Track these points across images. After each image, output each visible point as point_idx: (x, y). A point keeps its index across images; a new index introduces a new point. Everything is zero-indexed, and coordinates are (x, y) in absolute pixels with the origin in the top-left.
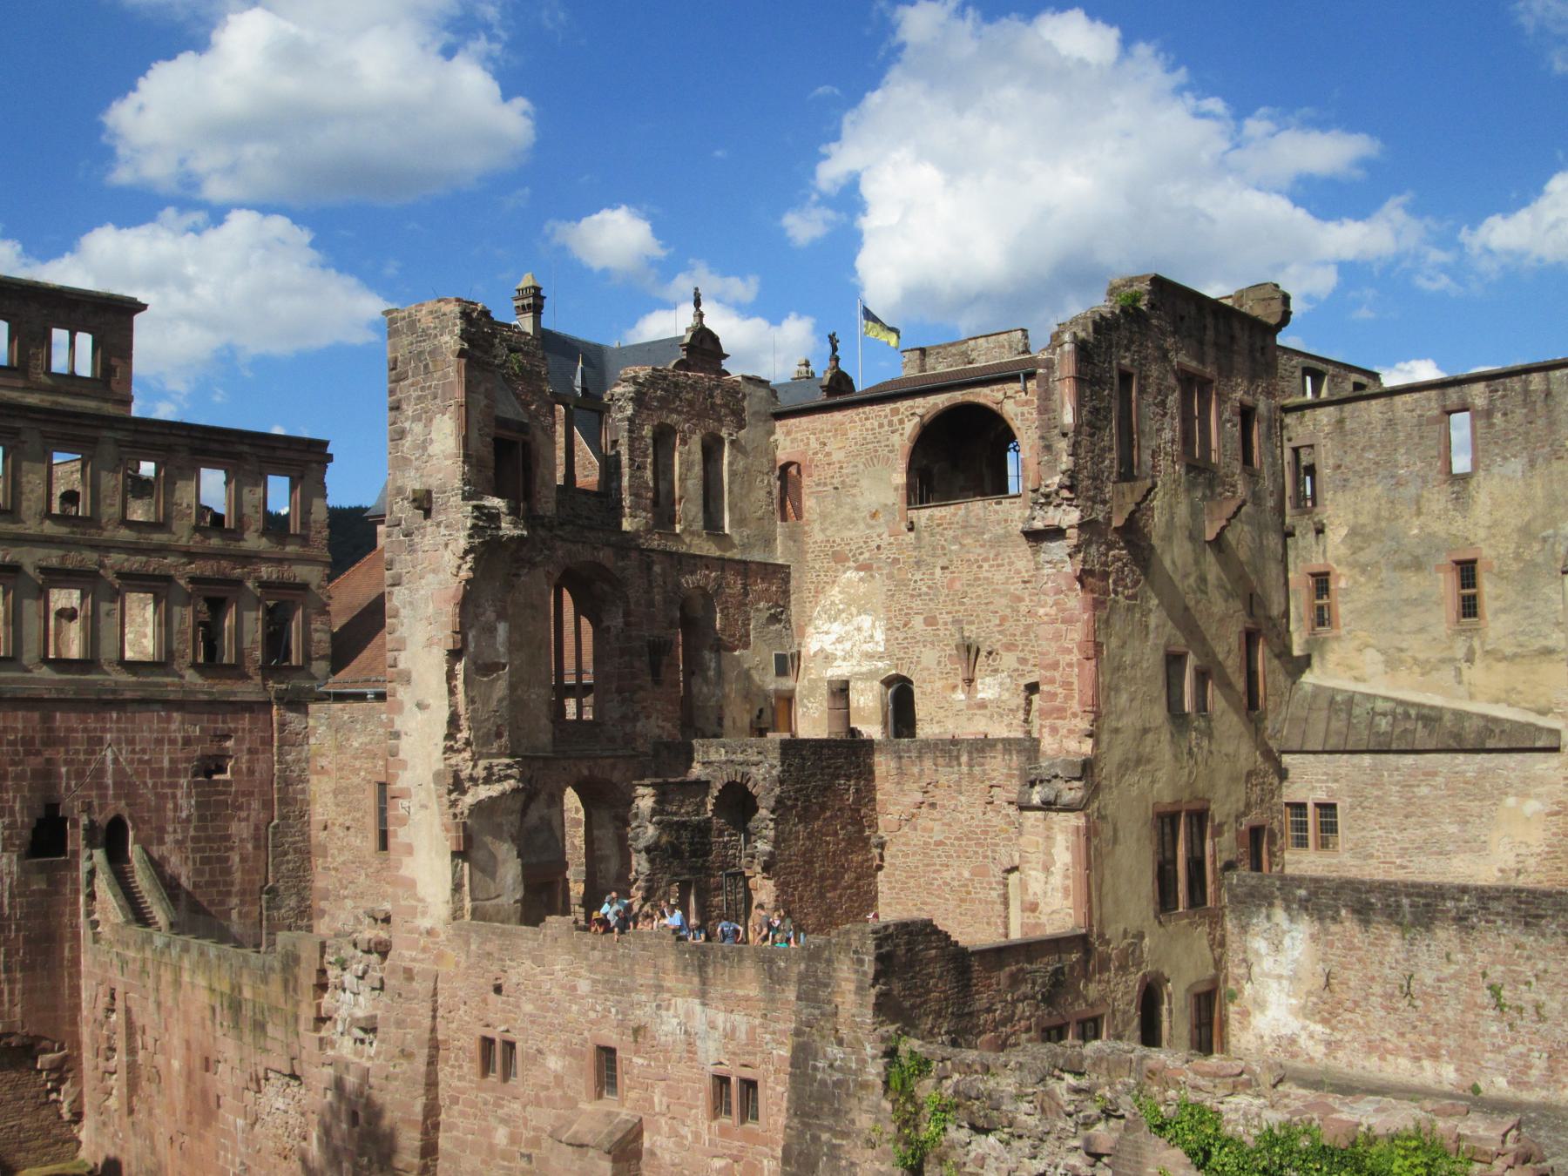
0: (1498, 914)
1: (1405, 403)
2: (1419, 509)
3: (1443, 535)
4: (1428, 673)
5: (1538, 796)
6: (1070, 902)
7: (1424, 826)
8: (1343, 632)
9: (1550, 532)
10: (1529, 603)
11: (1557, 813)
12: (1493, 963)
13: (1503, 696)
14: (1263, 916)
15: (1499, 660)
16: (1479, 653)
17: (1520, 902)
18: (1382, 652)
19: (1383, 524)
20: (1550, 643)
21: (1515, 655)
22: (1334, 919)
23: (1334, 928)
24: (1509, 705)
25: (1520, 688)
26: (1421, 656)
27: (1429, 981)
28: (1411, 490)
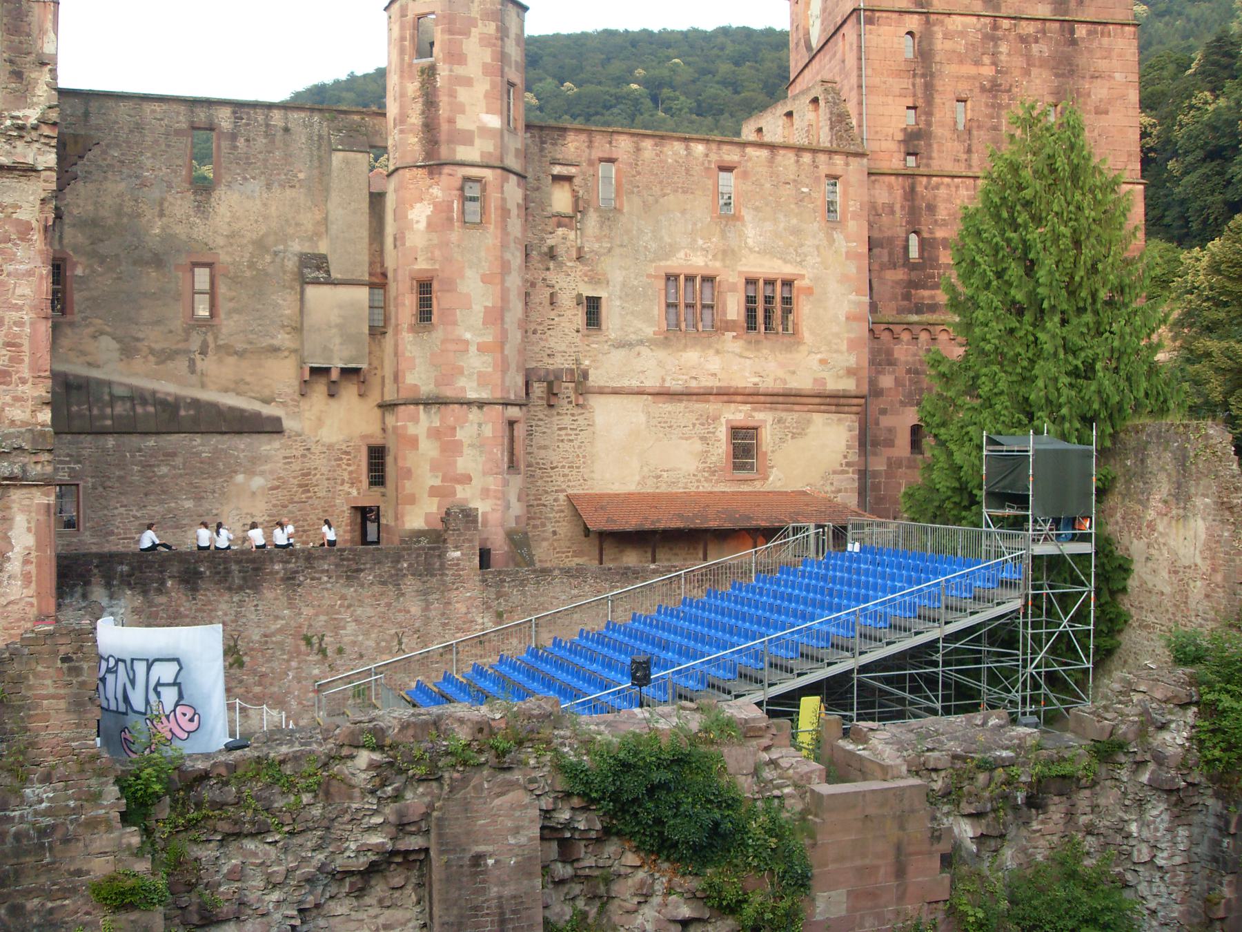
0: (323, 571)
1: (153, 111)
2: (162, 210)
3: (184, 237)
4: (163, 362)
5: (262, 473)
6: (32, 590)
7: (162, 502)
8: (77, 318)
9: (281, 247)
10: (260, 307)
11: (277, 488)
12: (317, 615)
13: (232, 386)
14: (77, 595)
15: (229, 354)
16: (212, 345)
17: (343, 560)
18: (118, 340)
19: (125, 220)
20: (276, 342)
21: (245, 351)
22: (160, 591)
23: (162, 599)
24: (238, 394)
25: (248, 379)
26: (157, 346)
27: (256, 638)
28: (156, 193)
